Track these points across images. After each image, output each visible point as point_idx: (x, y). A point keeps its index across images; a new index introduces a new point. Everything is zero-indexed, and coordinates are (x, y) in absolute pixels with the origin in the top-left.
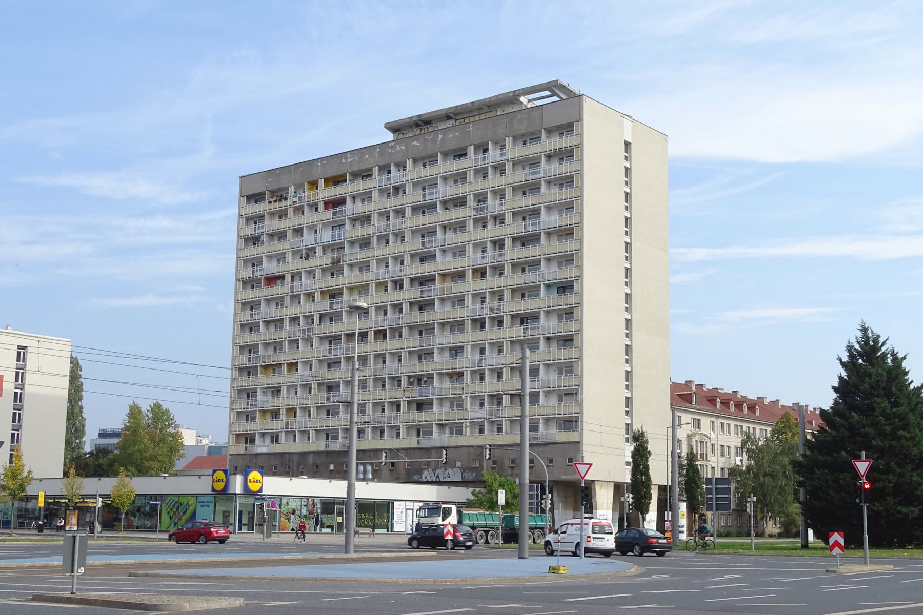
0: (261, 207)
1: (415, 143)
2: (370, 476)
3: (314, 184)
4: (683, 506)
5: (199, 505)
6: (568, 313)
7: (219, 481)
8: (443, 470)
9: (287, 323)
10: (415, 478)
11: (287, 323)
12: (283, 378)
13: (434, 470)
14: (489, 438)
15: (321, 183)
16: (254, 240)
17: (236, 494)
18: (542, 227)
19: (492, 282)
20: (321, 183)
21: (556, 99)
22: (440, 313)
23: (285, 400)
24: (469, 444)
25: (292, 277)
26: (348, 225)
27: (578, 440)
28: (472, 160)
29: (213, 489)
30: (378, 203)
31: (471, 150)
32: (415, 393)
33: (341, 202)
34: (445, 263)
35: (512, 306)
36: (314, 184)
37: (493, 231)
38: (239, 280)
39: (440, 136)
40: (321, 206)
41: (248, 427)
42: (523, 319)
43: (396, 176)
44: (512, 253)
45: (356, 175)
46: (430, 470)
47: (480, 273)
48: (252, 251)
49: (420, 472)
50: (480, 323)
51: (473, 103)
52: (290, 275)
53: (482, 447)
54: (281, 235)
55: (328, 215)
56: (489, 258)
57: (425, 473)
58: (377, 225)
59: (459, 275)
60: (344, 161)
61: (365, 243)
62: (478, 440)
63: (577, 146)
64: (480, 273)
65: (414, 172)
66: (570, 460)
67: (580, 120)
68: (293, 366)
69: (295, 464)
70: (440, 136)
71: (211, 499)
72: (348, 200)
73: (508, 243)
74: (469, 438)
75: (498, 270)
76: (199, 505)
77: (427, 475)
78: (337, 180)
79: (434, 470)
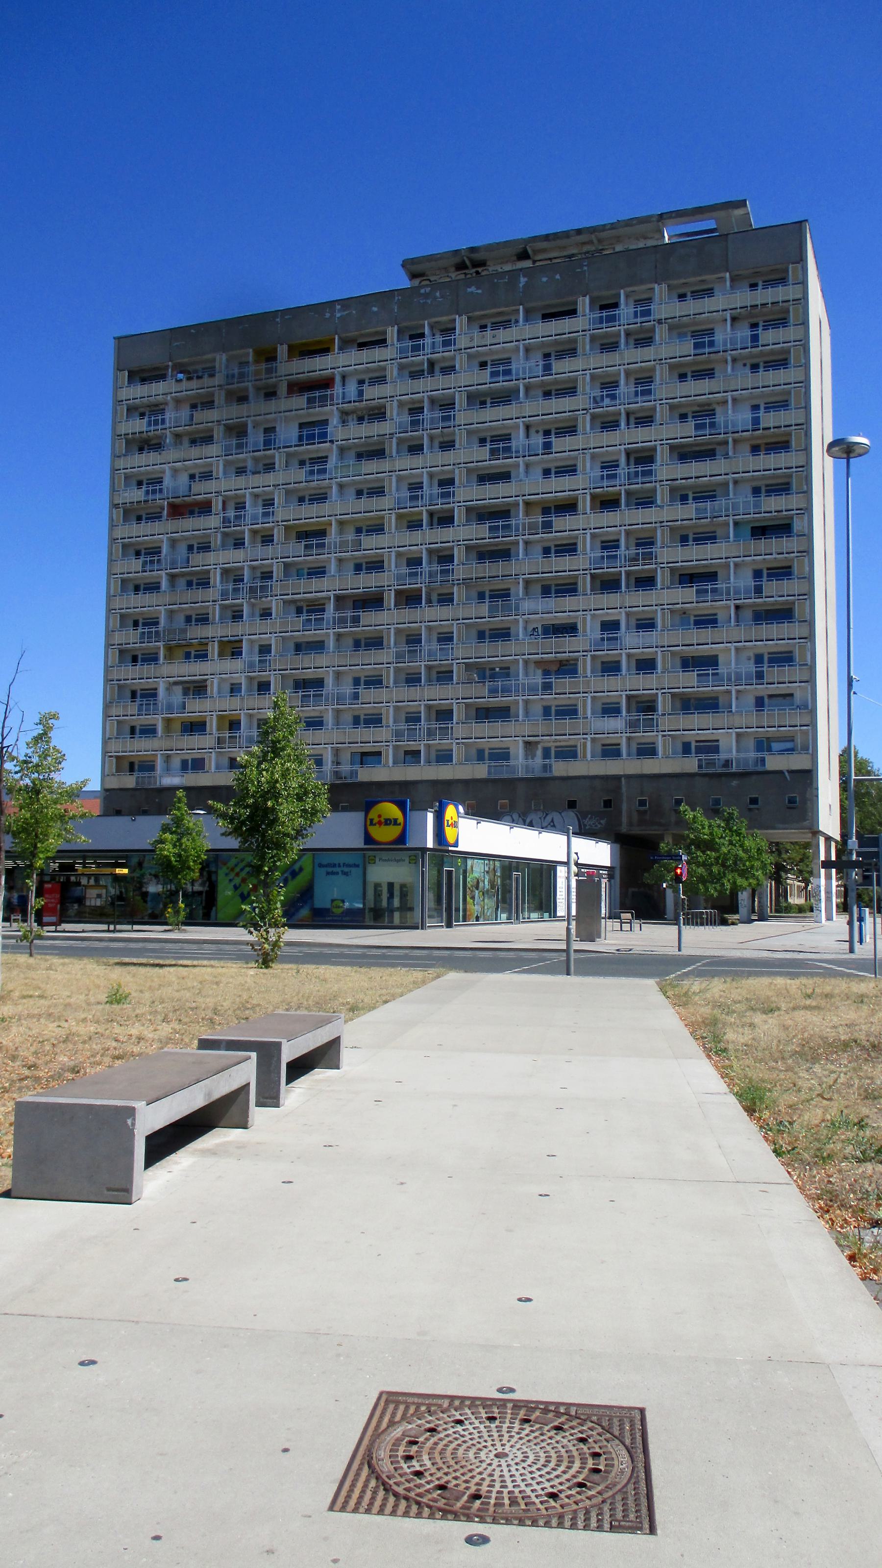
0: (157, 390)
1: (473, 289)
7: (389, 822)
8: (540, 814)
14: (627, 766)
15: (282, 351)
16: (145, 444)
17: (424, 850)
20: (282, 351)
24: (592, 773)
25: (224, 503)
29: (368, 839)
31: (584, 303)
32: (482, 694)
34: (528, 485)
38: (116, 506)
39: (523, 280)
41: (141, 747)
45: (346, 344)
46: (515, 816)
48: (144, 462)
52: (220, 499)
53: (617, 778)
59: (568, 507)
60: (328, 315)
62: (612, 767)
70: (523, 280)
72: (338, 379)
73: (662, 455)
74: (589, 766)
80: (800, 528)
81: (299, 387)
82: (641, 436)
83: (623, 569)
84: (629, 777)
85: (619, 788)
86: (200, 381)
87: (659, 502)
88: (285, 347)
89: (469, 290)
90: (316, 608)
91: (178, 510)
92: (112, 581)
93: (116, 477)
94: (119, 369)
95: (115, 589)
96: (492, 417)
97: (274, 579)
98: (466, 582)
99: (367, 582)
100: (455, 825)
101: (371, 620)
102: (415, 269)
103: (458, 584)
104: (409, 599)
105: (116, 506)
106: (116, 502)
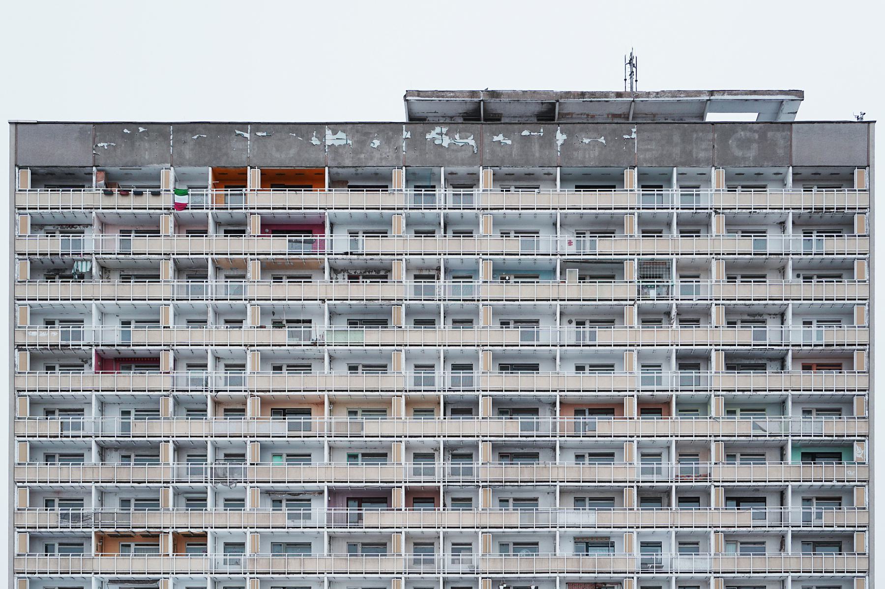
1: (500, 137)
3: (230, 179)
11: (168, 453)
15: (254, 177)
20: (254, 177)
22: (563, 469)
28: (628, 197)
35: (726, 473)
36: (230, 179)
38: (20, 347)
40: (254, 225)
44: (717, 378)
50: (651, 498)
58: (400, 288)
67: (867, 165)
75: (694, 408)
80: (860, 456)
82: (693, 337)
83: (674, 485)
86: (139, 198)
87: (713, 414)
88: (258, 172)
89: (496, 138)
90: (298, 499)
91: (111, 361)
92: (17, 445)
93: (18, 308)
94: (18, 166)
97: (248, 462)
98: (495, 486)
103: (483, 487)
104: (421, 497)
105: (20, 347)
106: (20, 340)
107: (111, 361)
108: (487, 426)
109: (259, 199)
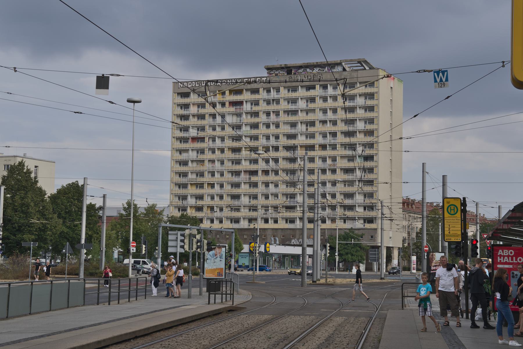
2: (278, 242)
4: (414, 258)
5: (240, 258)
6: (371, 170)
9: (206, 162)
10: (287, 243)
12: (206, 191)
13: (298, 239)
15: (227, 93)
18: (358, 129)
19: (329, 152)
20: (227, 93)
21: (362, 68)
23: (207, 201)
26: (244, 116)
27: (376, 227)
28: (318, 92)
29: (250, 250)
30: (263, 107)
33: (240, 103)
37: (329, 127)
38: (174, 137)
40: (227, 104)
42: (347, 171)
43: (273, 94)
47: (323, 147)
49: (290, 240)
51: (317, 63)
53: (325, 229)
54: (202, 117)
55: (232, 109)
56: (329, 140)
57: (293, 241)
58: (263, 118)
61: (255, 126)
63: (376, 93)
64: (323, 147)
65: (284, 93)
66: (372, 237)
68: (212, 186)
69: (214, 234)
71: (248, 255)
72: (244, 103)
75: (334, 147)
76: (240, 258)
77: (293, 241)
78: (239, 92)
79: (298, 239)
81: (233, 104)
84: (327, 229)
85: (325, 232)
90: (237, 173)
91: (195, 139)
95: (174, 165)
96: (292, 118)
99: (253, 167)
100: (269, 247)
101: (254, 179)
102: (269, 69)
105: (174, 137)
107: (194, 139)
108: (282, 153)
109: (229, 98)
